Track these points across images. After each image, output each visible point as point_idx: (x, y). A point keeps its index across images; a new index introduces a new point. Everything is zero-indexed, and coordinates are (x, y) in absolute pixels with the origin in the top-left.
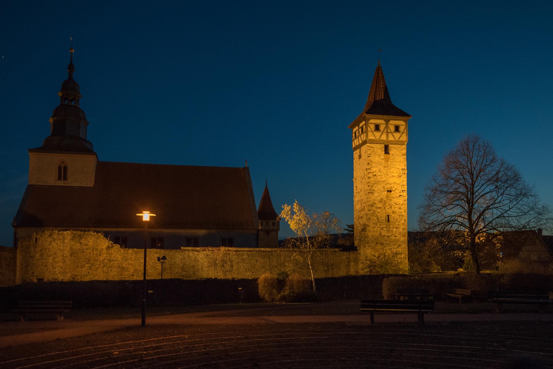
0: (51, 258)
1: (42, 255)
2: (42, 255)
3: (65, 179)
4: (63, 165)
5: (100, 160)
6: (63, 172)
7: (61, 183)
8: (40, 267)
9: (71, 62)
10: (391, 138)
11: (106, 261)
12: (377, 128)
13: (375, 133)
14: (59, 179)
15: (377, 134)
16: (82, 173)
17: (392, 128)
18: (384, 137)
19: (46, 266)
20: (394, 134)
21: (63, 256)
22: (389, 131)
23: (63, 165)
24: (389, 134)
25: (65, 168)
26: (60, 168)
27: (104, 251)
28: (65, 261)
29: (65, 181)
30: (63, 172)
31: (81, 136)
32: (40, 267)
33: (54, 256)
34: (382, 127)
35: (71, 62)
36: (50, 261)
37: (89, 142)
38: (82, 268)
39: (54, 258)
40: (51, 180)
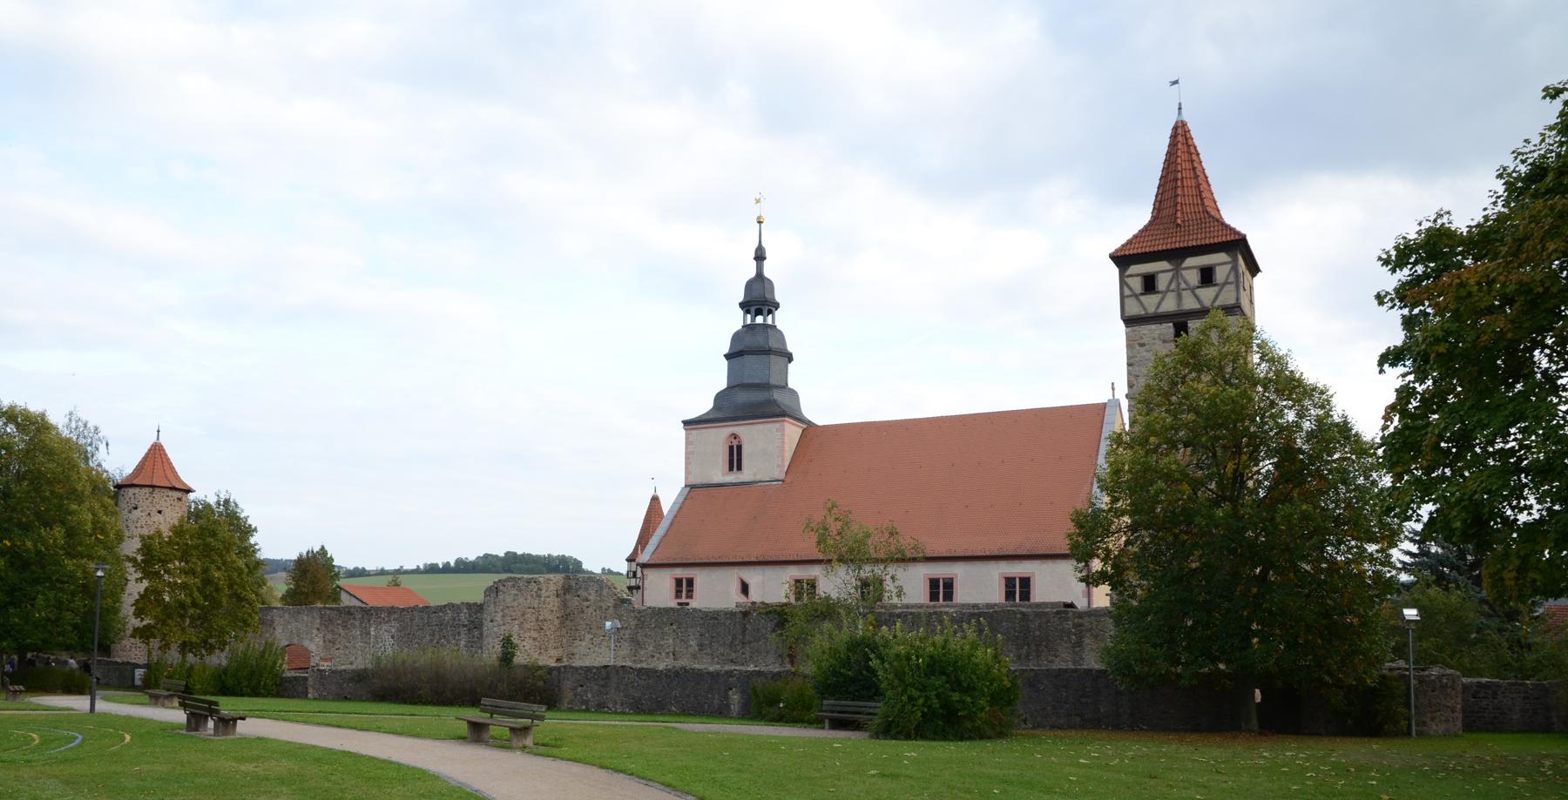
3: (739, 468)
6: (735, 458)
10: (1190, 303)
12: (1149, 283)
13: (1142, 298)
14: (731, 469)
15: (1151, 303)
16: (770, 450)
17: (1193, 277)
18: (1169, 305)
20: (1198, 291)
22: (1183, 286)
23: (735, 443)
24: (1186, 295)
25: (739, 448)
26: (731, 448)
27: (611, 611)
30: (735, 458)
31: (773, 382)
34: (1162, 282)
37: (794, 393)
40: (719, 474)
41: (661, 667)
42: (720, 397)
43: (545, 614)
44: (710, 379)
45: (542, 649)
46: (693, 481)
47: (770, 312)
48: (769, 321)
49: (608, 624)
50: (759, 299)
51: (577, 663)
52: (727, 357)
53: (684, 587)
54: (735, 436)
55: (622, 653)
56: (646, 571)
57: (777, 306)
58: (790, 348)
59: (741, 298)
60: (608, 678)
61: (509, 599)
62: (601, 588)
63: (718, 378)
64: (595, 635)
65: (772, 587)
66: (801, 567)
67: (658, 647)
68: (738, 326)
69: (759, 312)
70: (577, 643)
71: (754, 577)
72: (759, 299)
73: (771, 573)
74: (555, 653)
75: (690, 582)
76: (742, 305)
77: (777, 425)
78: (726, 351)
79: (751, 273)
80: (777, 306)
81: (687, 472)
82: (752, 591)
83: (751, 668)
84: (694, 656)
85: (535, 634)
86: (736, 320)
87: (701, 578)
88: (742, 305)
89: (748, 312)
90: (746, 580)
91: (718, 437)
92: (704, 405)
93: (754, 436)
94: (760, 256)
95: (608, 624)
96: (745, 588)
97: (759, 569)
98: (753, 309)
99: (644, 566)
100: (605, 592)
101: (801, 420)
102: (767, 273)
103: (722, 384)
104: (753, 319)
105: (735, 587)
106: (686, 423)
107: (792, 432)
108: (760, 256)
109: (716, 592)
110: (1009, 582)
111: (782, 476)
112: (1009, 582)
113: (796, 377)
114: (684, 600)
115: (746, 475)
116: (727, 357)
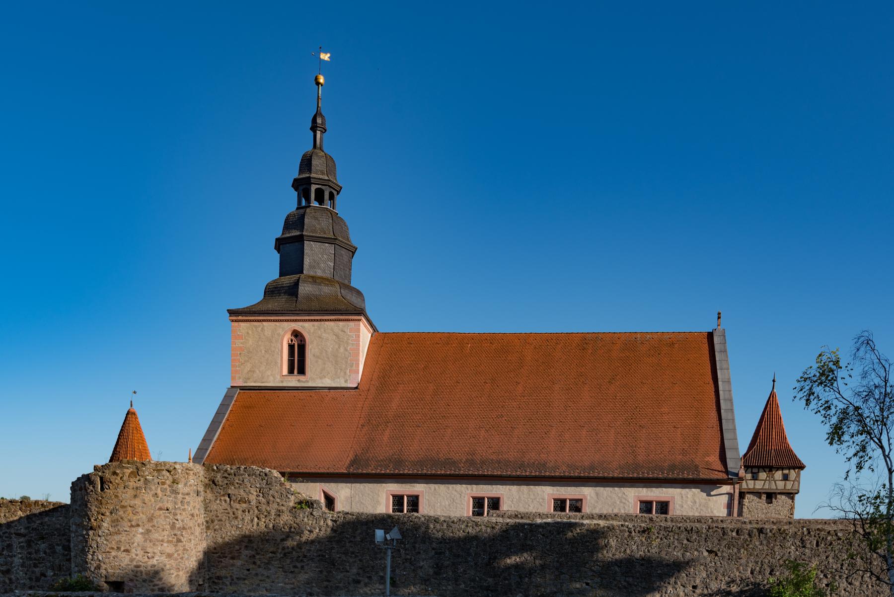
0: (140, 530)
1: (115, 522)
2: (115, 522)
3: (302, 371)
5: (382, 329)
8: (113, 553)
14: (291, 371)
19: (127, 551)
21: (173, 527)
26: (291, 347)
28: (179, 541)
29: (302, 378)
32: (113, 553)
33: (148, 526)
36: (139, 538)
37: (359, 293)
38: (233, 558)
39: (148, 531)
40: (277, 373)
43: (183, 518)
54: (296, 334)
77: (352, 324)
85: (169, 549)
90: (332, 493)
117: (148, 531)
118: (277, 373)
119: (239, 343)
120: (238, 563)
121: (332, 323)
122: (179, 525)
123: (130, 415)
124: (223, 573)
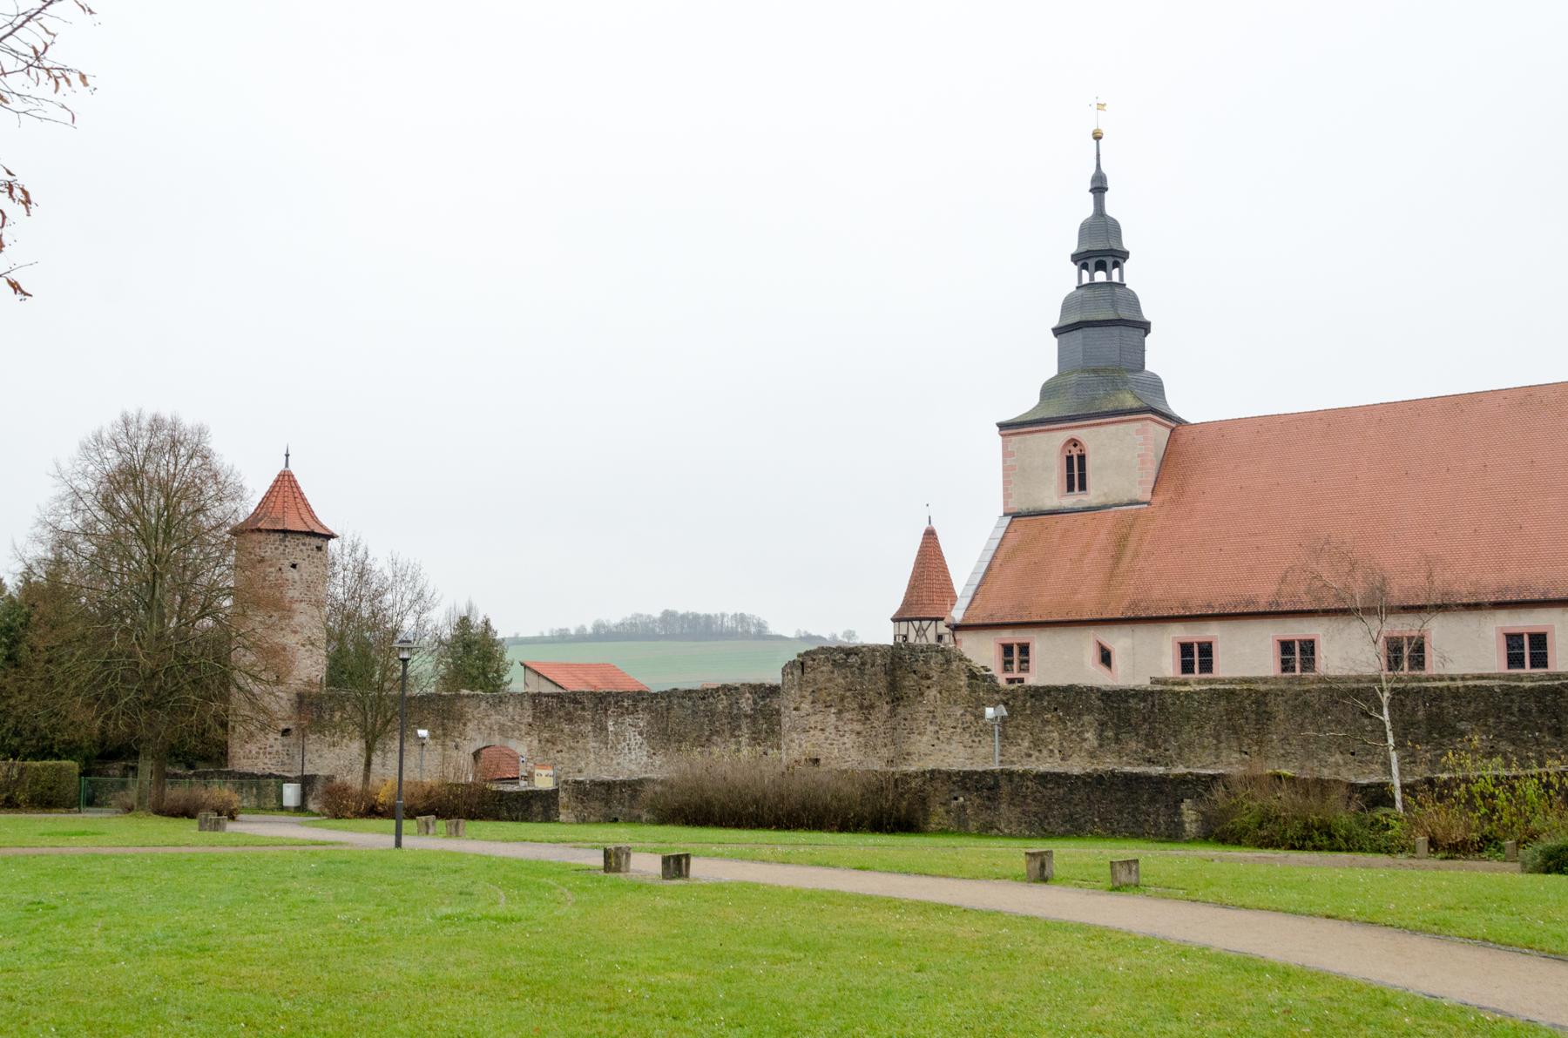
3: (1083, 487)
4: (1075, 452)
6: (1076, 472)
7: (1071, 501)
9: (1098, 165)
11: (969, 717)
14: (1070, 488)
21: (861, 707)
23: (1075, 452)
25: (1082, 458)
26: (1070, 459)
30: (1076, 472)
35: (1098, 165)
40: (1052, 494)
41: (1076, 771)
42: (1048, 391)
44: (1031, 365)
45: (868, 747)
46: (1016, 507)
47: (1116, 265)
48: (1116, 279)
49: (990, 712)
50: (1101, 250)
51: (913, 767)
52: (1058, 332)
53: (1018, 655)
54: (1075, 443)
55: (982, 751)
56: (959, 635)
57: (1125, 255)
58: (1147, 316)
59: (1073, 247)
60: (997, 786)
61: (821, 678)
62: (948, 661)
63: (1044, 360)
64: (941, 727)
65: (1145, 660)
66: (1190, 625)
67: (1037, 744)
68: (1071, 286)
69: (1100, 266)
70: (915, 737)
71: (1120, 641)
72: (1101, 250)
73: (1143, 633)
74: (885, 753)
75: (1024, 649)
76: (1076, 258)
77: (1138, 425)
78: (1055, 322)
79: (1087, 209)
80: (1125, 255)
81: (1007, 496)
82: (1116, 659)
83: (1180, 770)
84: (1092, 755)
85: (858, 727)
86: (1069, 278)
87: (1040, 643)
88: (1076, 258)
89: (1084, 266)
90: (1108, 644)
91: (1052, 444)
92: (1025, 401)
93: (1098, 441)
94: (1099, 188)
95: (990, 712)
96: (1106, 658)
97: (1127, 628)
98: (1091, 263)
99: (956, 628)
100: (954, 666)
101: (1169, 417)
102: (1111, 210)
103: (1052, 371)
104: (1092, 277)
105: (1091, 655)
106: (1002, 426)
107: (1158, 433)
108: (1099, 188)
109: (1061, 662)
110: (1513, 640)
111: (1148, 497)
112: (1513, 640)
113: (1158, 356)
114: (1016, 675)
115: (1092, 496)
116: (1058, 332)
117: (840, 712)
118: (1052, 494)
119: (1010, 461)
120: (925, 739)
121: (1112, 428)
122: (866, 703)
123: (930, 534)
124: (912, 749)
